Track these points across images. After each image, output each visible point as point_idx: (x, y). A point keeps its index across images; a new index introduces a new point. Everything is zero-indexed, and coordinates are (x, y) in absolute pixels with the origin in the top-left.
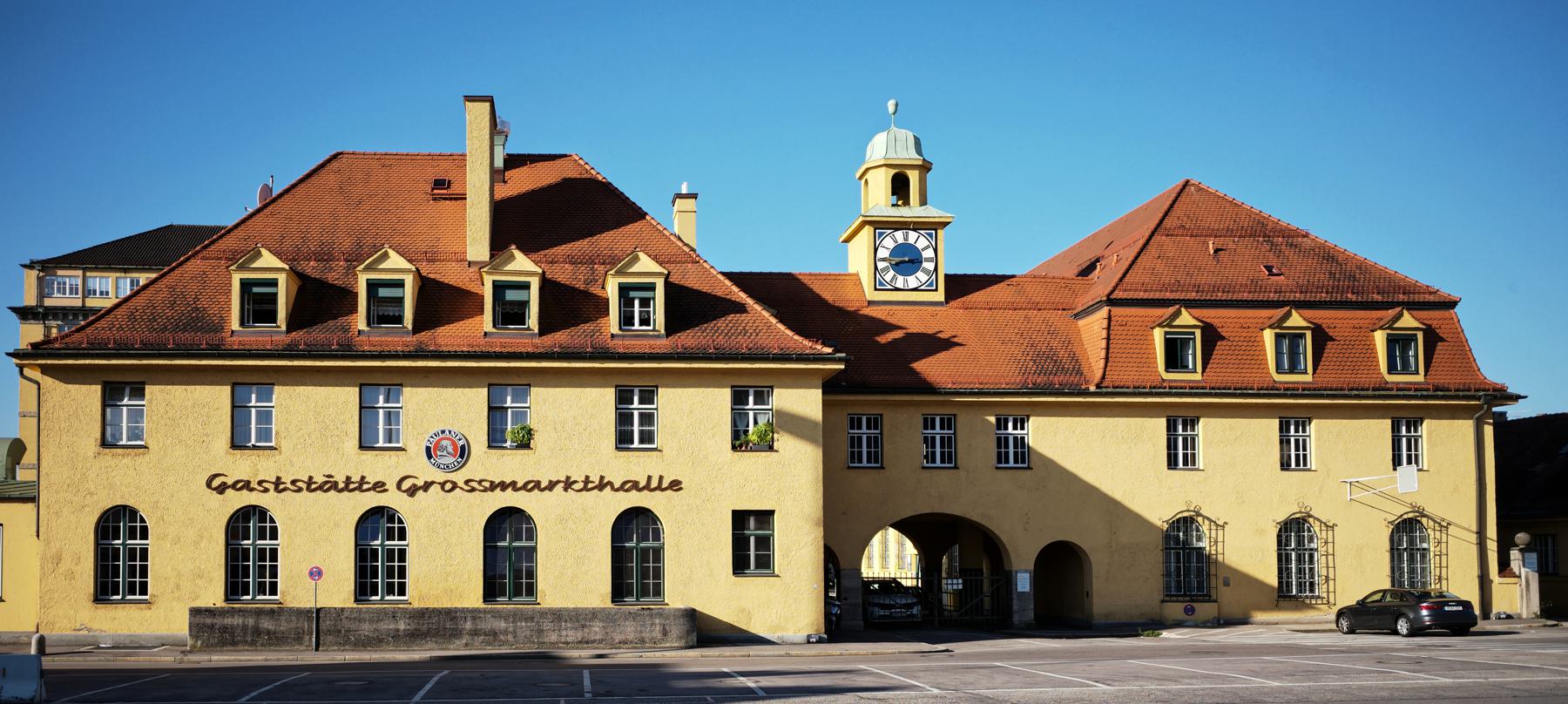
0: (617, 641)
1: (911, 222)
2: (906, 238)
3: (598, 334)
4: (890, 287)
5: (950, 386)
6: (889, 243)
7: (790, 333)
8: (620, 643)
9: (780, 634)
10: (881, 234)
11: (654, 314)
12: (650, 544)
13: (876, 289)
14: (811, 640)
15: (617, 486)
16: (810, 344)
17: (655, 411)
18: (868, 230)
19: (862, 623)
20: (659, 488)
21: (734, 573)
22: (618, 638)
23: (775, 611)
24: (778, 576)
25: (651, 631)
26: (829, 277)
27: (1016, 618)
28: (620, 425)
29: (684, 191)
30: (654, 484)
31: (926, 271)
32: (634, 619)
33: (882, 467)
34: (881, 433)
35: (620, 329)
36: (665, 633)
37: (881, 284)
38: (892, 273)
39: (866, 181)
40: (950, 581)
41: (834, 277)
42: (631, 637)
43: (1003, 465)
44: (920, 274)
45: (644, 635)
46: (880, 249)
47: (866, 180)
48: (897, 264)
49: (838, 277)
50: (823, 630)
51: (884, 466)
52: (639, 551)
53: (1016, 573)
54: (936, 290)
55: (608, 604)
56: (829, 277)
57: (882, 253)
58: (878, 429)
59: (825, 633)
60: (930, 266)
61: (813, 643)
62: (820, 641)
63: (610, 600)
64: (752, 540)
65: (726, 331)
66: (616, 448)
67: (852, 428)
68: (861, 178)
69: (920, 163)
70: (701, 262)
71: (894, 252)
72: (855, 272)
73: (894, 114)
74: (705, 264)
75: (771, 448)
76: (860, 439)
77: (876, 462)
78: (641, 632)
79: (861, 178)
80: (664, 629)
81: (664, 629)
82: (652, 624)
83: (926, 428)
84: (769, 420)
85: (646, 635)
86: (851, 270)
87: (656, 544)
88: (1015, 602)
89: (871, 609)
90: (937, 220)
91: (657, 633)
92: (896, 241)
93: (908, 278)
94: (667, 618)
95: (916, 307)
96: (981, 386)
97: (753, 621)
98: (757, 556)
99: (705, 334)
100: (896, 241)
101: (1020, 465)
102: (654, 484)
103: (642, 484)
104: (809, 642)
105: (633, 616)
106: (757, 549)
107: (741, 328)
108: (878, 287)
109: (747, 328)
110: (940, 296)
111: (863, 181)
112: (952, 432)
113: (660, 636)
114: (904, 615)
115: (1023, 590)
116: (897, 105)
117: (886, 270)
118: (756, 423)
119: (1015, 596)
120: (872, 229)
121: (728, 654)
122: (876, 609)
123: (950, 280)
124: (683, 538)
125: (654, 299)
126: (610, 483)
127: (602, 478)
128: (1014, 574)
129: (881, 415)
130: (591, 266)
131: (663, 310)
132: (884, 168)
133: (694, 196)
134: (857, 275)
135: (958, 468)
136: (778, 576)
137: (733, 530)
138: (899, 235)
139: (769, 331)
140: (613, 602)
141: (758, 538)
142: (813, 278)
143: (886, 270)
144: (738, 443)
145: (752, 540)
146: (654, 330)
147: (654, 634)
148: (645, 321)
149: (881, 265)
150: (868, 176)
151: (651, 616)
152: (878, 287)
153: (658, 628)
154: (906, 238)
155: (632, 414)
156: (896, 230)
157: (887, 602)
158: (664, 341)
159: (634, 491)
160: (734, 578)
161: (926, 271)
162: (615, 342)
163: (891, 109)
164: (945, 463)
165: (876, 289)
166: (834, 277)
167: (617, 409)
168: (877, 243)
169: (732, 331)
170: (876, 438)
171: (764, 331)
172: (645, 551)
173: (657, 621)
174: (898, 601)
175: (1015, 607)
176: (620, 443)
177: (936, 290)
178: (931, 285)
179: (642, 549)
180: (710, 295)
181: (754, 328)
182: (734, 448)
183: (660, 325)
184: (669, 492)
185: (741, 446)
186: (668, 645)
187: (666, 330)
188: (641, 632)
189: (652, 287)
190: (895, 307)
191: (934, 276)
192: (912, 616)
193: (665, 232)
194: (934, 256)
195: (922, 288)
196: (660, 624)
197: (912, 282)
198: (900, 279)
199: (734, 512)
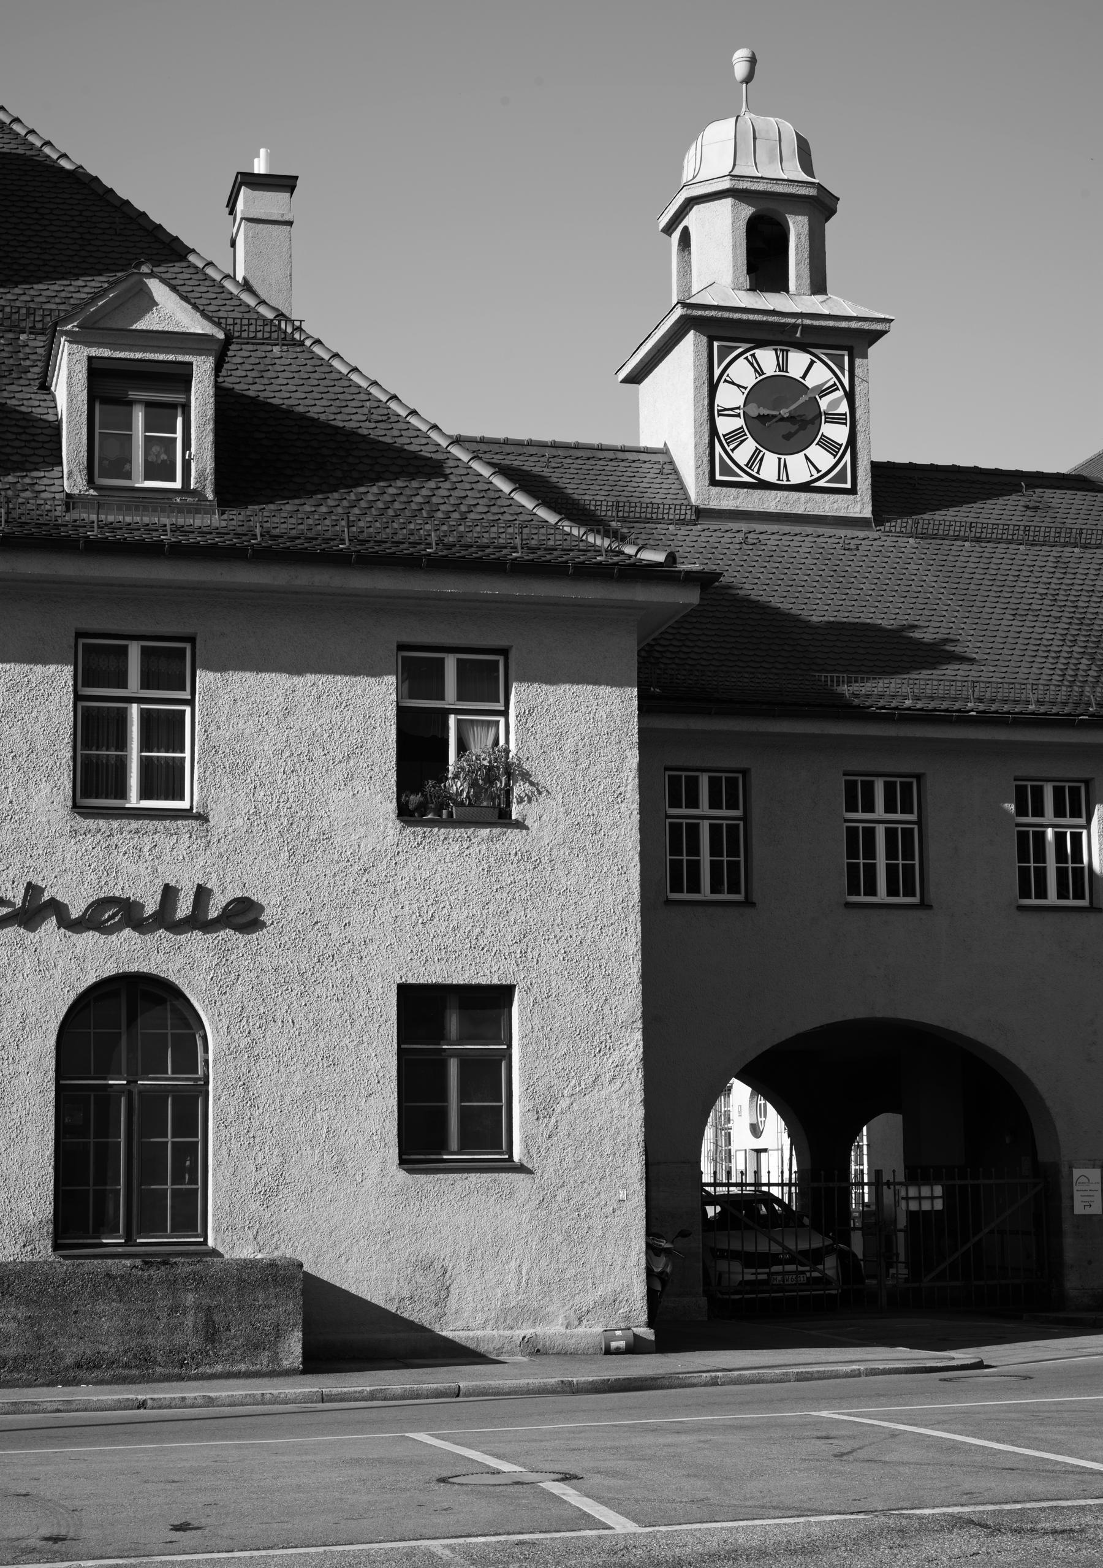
0: (69, 1360)
1: (795, 326)
2: (783, 366)
3: (28, 494)
4: (746, 479)
5: (908, 703)
6: (742, 372)
7: (551, 518)
8: (78, 1366)
9: (529, 1332)
10: (724, 353)
11: (187, 445)
12: (169, 1079)
13: (714, 482)
14: (614, 1345)
15: (75, 913)
16: (607, 542)
17: (188, 710)
18: (689, 346)
19: (703, 1301)
20: (198, 922)
21: (402, 1162)
22: (72, 1351)
23: (513, 1264)
24: (521, 1169)
25: (172, 1329)
26: (600, 454)
27: (1072, 1283)
28: (86, 745)
29: (260, 166)
30: (184, 908)
31: (829, 445)
32: (119, 1290)
33: (748, 903)
34: (745, 818)
35: (91, 481)
36: (211, 1333)
37: (726, 470)
38: (750, 445)
39: (686, 233)
40: (913, 1192)
41: (611, 455)
42: (111, 1347)
43: (1033, 902)
44: (815, 451)
45: (150, 1340)
46: (723, 387)
47: (686, 230)
48: (760, 417)
49: (621, 455)
50: (644, 1318)
51: (756, 897)
52: (136, 1097)
53: (1071, 1167)
54: (853, 491)
55: (44, 1250)
56: (600, 454)
57: (728, 397)
58: (735, 807)
59: (650, 1324)
60: (838, 433)
61: (618, 1352)
62: (636, 1347)
63: (49, 1243)
64: (453, 1066)
65: (380, 505)
66: (75, 806)
67: (675, 803)
68: (669, 229)
69: (812, 192)
70: (308, 343)
71: (753, 395)
72: (661, 446)
73: (748, 80)
74: (317, 349)
75: (502, 818)
76: (694, 830)
77: (734, 888)
78: (141, 1332)
79: (669, 229)
80: (209, 1321)
81: (209, 1321)
82: (174, 1309)
83: (851, 807)
84: (496, 742)
85: (157, 1342)
86: (648, 439)
87: (182, 1081)
88: (1069, 1241)
89: (723, 1265)
90: (854, 325)
91: (189, 1337)
92: (759, 371)
93: (788, 458)
94: (219, 1290)
95: (809, 530)
96: (982, 707)
97: (453, 1297)
98: (464, 1113)
99: (323, 509)
100: (759, 371)
101: (1071, 902)
102: (184, 908)
103: (151, 907)
104: (608, 1351)
105: (120, 1286)
106: (464, 1095)
107: (418, 499)
108: (718, 477)
109: (435, 500)
110: (861, 506)
111: (676, 235)
112: (913, 817)
113: (195, 1343)
114: (790, 1280)
115: (1088, 1211)
116: (753, 61)
117: (736, 437)
118: (462, 747)
119: (1067, 1226)
120: (704, 339)
121: (397, 1388)
122: (736, 1266)
123: (882, 471)
124: (262, 1062)
125: (186, 408)
126: (57, 908)
127: (32, 890)
128: (1065, 1170)
129: (745, 772)
130: (10, 335)
131: (210, 439)
132: (728, 202)
133: (285, 183)
134: (665, 451)
135: (930, 907)
136: (521, 1169)
137: (400, 1042)
138: (767, 358)
139: (494, 509)
140: (56, 1247)
141: (468, 1063)
142: (560, 452)
143: (736, 437)
144: (415, 799)
145: (453, 1066)
146: (185, 490)
147: (179, 1339)
148: (160, 468)
149: (724, 425)
150: (691, 220)
151: (172, 1284)
152: (718, 477)
153: (190, 1320)
154: (783, 366)
155: (122, 718)
156: (761, 344)
157: (763, 1247)
158: (215, 520)
159: (127, 932)
160: (402, 1176)
161: (829, 445)
162: (75, 515)
163: (740, 69)
164: (897, 894)
165: (714, 482)
166: (611, 455)
167: (78, 698)
168: (717, 372)
169: (397, 505)
170: (733, 830)
171: (480, 509)
172: (156, 1097)
173: (190, 1298)
174: (791, 1244)
175: (1069, 1256)
176: (86, 794)
177: (853, 491)
178: (840, 478)
179: (145, 1092)
180: (326, 425)
181: (452, 501)
182: (406, 814)
183: (201, 475)
184: (225, 934)
185: (422, 809)
186: (219, 1368)
187: (217, 492)
188: (141, 1332)
189: (182, 378)
190: (760, 527)
191: (847, 457)
192: (824, 1281)
193: (210, 271)
194: (844, 408)
195: (821, 483)
196: (198, 1308)
197: (798, 469)
198: (771, 460)
199: (406, 992)
